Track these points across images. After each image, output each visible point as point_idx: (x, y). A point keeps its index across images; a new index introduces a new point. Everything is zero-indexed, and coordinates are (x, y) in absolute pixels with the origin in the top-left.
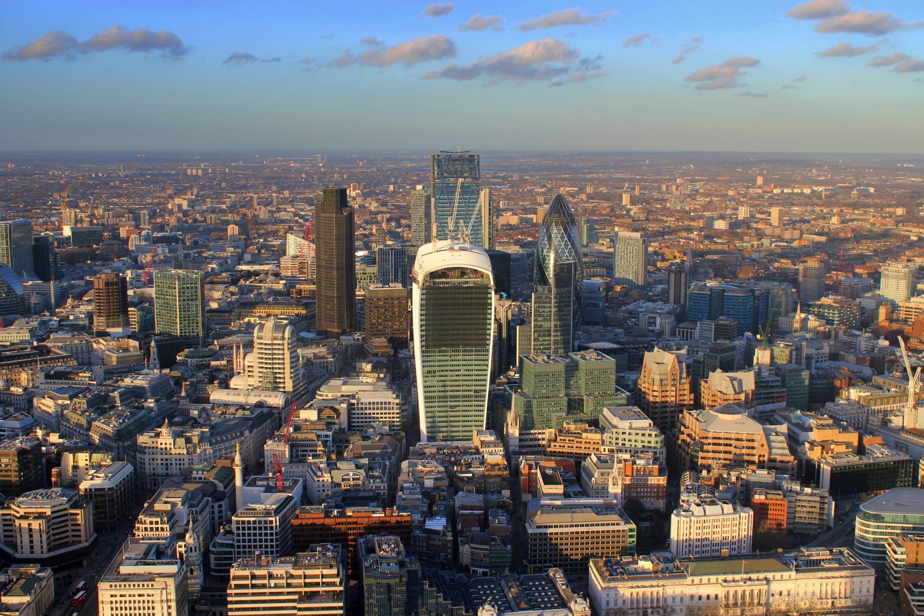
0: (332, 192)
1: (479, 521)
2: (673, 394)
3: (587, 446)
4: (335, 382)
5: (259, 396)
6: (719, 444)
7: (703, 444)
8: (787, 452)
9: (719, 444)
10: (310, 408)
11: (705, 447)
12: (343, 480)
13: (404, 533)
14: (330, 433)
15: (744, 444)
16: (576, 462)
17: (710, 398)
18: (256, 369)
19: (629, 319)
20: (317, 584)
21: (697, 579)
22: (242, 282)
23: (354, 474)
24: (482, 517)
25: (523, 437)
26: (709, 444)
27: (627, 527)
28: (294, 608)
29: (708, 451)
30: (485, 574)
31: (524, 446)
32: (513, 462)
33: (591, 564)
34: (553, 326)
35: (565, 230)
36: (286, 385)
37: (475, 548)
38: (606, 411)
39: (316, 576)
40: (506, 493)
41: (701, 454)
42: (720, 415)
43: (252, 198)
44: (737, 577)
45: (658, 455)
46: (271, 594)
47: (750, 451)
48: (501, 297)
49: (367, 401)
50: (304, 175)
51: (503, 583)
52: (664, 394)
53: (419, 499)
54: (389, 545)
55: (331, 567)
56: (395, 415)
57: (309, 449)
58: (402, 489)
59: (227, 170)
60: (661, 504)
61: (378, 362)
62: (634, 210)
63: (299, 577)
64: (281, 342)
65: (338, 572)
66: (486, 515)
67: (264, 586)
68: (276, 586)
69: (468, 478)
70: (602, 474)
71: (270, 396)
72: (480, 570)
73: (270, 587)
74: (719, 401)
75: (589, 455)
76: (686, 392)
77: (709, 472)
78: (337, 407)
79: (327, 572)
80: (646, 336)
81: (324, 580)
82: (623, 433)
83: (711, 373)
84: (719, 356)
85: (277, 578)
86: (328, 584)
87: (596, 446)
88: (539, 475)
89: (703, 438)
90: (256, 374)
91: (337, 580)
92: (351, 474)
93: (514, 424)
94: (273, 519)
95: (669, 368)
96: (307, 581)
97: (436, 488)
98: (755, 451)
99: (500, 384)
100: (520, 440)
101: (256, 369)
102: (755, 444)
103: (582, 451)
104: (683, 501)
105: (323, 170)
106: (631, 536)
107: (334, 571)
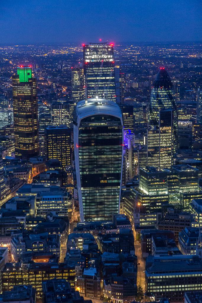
53: (79, 257)
54: (62, 286)
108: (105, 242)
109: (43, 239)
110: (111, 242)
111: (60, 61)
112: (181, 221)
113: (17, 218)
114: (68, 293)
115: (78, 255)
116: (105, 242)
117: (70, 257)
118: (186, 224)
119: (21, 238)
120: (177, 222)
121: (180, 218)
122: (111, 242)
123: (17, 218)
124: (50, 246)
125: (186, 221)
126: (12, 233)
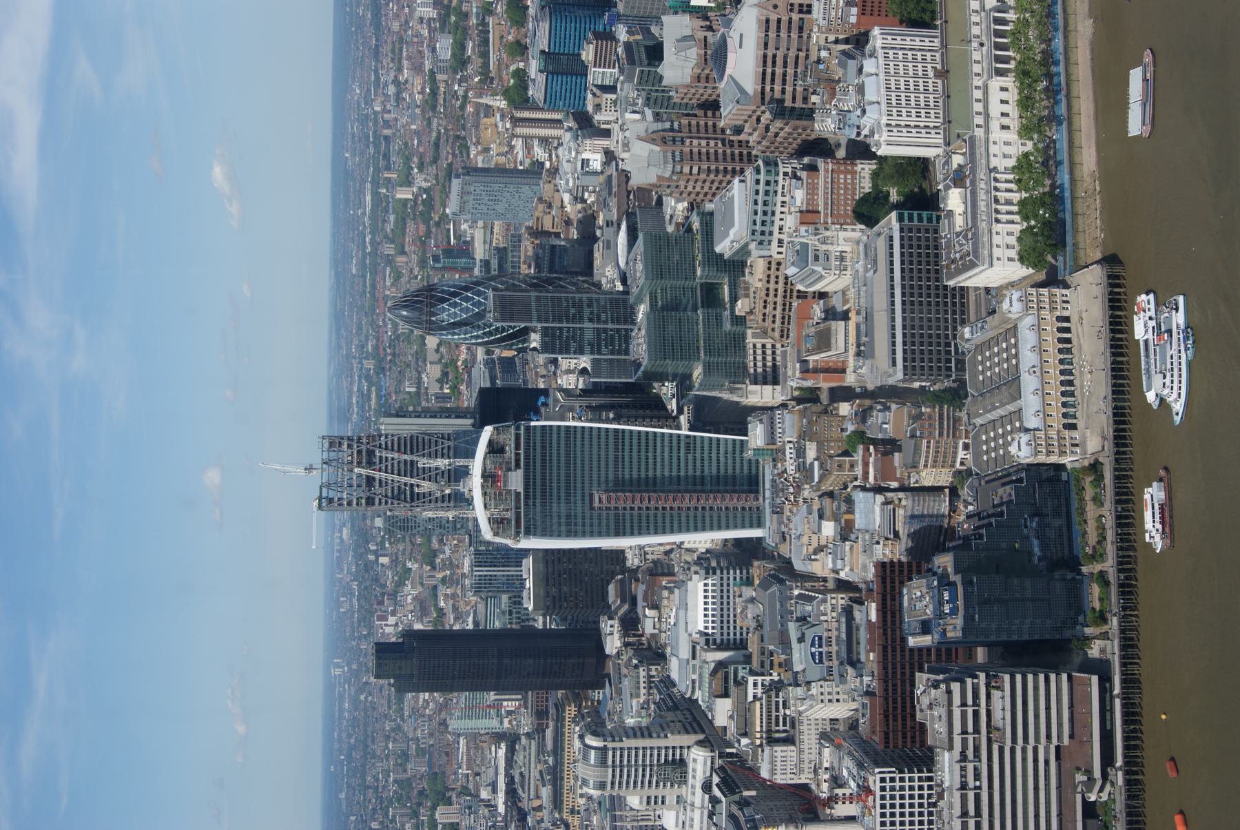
0: (379, 665)
1: (885, 454)
2: (695, 142)
3: (773, 279)
5: (693, 787)
6: (773, 74)
7: (772, 99)
9: (773, 74)
10: (711, 710)
11: (777, 95)
13: (901, 571)
14: (751, 680)
15: (772, 34)
16: (798, 297)
17: (702, 84)
18: (653, 792)
19: (583, 201)
20: (976, 714)
21: (979, 120)
22: (525, 804)
24: (881, 448)
26: (772, 90)
27: (896, 226)
28: (1013, 750)
29: (783, 92)
30: (966, 447)
33: (951, 283)
35: (443, 300)
36: (677, 744)
37: (926, 461)
38: (718, 249)
39: (964, 715)
40: (845, 408)
41: (788, 103)
42: (728, 71)
43: (395, 781)
44: (976, 56)
45: (789, 170)
46: (990, 787)
47: (784, 26)
48: (545, 404)
49: (701, 618)
50: (362, 697)
51: (979, 421)
52: (696, 157)
53: (852, 547)
55: (949, 692)
56: (725, 576)
57: (774, 714)
59: (353, 818)
60: (865, 169)
61: (645, 599)
62: (421, 181)
63: (964, 742)
64: (610, 753)
65: (955, 680)
66: (874, 442)
67: (977, 798)
68: (977, 776)
69: (821, 467)
70: (817, 258)
71: (694, 770)
72: (961, 454)
73: (979, 788)
74: (707, 71)
75: (786, 278)
76: (694, 122)
78: (713, 665)
79: (957, 700)
80: (610, 177)
81: (970, 702)
82: (755, 223)
83: (664, 83)
85: (963, 776)
86: (976, 695)
87: (774, 266)
88: (816, 357)
89: (763, 99)
90: (660, 792)
91: (969, 681)
92: (813, 650)
94: (878, 776)
95: (657, 148)
96: (970, 729)
98: (785, 19)
99: (680, 411)
100: (765, 383)
101: (653, 792)
102: (774, 17)
104: (858, 134)
105: (354, 667)
106: (911, 219)
107: (956, 687)
108: (816, 479)
109: (803, 634)
110: (816, 463)
111: (372, 557)
112: (768, 282)
113: (750, 698)
114: (936, 583)
115: (847, 548)
116: (816, 479)
117: (852, 570)
119: (799, 691)
120: (772, 293)
121: (759, 285)
122: (816, 463)
123: (750, 698)
124: (822, 618)
125: (769, 269)
126: (788, 712)
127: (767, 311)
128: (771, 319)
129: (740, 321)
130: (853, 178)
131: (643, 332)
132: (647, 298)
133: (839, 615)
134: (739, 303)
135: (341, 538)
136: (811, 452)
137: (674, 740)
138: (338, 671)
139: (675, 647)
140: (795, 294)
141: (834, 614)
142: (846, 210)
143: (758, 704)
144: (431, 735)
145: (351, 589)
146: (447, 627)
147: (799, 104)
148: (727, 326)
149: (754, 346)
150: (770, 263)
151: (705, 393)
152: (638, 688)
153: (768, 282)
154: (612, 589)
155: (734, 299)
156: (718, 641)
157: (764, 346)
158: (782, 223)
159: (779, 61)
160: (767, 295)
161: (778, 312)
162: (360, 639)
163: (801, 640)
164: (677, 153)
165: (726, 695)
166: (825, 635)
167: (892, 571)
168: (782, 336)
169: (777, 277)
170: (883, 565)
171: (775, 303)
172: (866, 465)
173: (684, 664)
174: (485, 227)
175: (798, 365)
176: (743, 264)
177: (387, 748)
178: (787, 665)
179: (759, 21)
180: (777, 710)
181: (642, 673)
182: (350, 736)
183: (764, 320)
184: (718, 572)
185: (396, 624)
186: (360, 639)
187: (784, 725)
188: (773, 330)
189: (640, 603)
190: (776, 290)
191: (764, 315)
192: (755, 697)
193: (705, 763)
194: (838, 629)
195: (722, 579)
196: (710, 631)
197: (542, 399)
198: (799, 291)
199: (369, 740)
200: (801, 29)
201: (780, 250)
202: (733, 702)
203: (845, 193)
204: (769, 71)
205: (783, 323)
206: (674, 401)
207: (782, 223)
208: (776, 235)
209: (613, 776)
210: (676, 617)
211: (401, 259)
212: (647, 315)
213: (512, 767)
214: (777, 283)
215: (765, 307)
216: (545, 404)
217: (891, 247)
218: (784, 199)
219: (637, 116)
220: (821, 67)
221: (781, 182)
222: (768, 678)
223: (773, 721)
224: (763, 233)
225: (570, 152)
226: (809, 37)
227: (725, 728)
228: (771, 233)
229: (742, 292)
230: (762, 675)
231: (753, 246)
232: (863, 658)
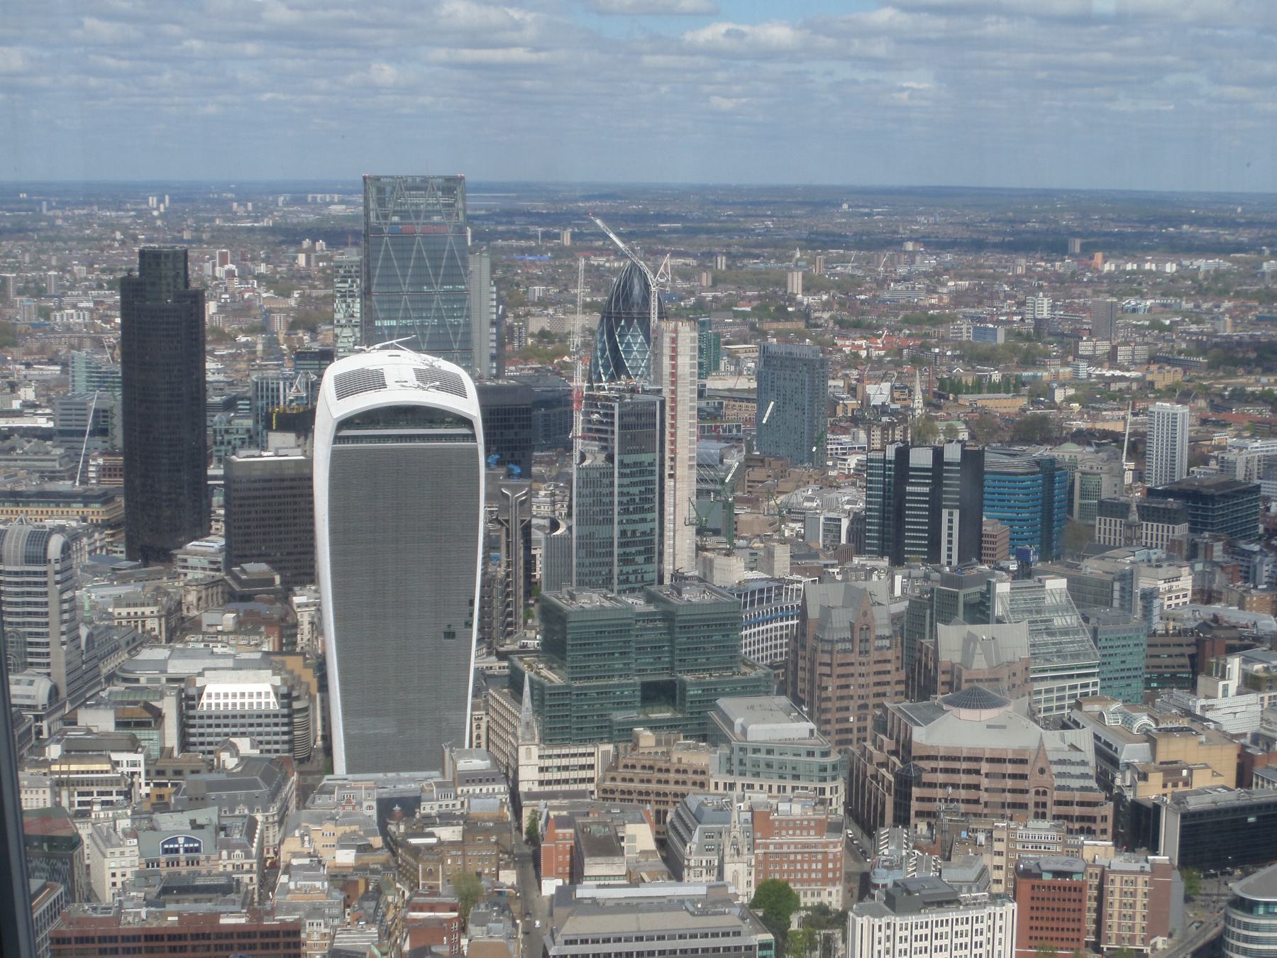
3: (681, 777)
4: (160, 653)
8: (1093, 783)
9: (954, 771)
10: (98, 705)
12: (166, 851)
14: (140, 757)
16: (658, 812)
23: (188, 840)
24: (456, 926)
25: (548, 763)
26: (934, 770)
29: (931, 785)
31: (549, 782)
32: (526, 813)
34: (616, 534)
57: (95, 789)
58: (288, 869)
60: (834, 897)
69: (430, 848)
75: (683, 796)
77: (929, 825)
80: (816, 556)
82: (756, 751)
83: (940, 626)
84: (962, 593)
87: (699, 778)
92: (181, 840)
93: (528, 737)
97: (360, 868)
100: (541, 769)
103: (671, 788)
105: (159, 223)
108: (414, 841)
110: (433, 841)
112: (678, 771)
113: (115, 757)
116: (414, 841)
118: (694, 783)
120: (663, 776)
121: (675, 759)
123: (115, 757)
124: (224, 853)
125: (695, 772)
126: (97, 808)
127: (638, 770)
128: (628, 776)
129: (624, 734)
130: (816, 881)
131: (607, 604)
132: (652, 608)
133: (228, 875)
134: (648, 733)
135: (332, 203)
136: (449, 834)
137: (59, 654)
138: (153, 201)
139: (184, 654)
140: (662, 807)
141: (230, 868)
142: (775, 872)
143: (107, 767)
144: (68, 328)
145: (263, 216)
146: (208, 348)
147: (915, 806)
148: (619, 716)
149: (592, 754)
150: (703, 773)
151: (527, 689)
152: (128, 605)
153: (678, 771)
154: (263, 567)
155: (654, 726)
156: (192, 712)
157: (591, 767)
158: (757, 787)
159: (972, 779)
160: (660, 770)
161: (636, 786)
162: (196, 230)
163: (195, 825)
164: (848, 646)
165: (119, 724)
166: (202, 857)
167: (288, 945)
168: (605, 791)
169: (684, 783)
170: (297, 933)
171: (649, 781)
172: (432, 908)
173: (161, 666)
174: (749, 391)
175: (564, 813)
176: (704, 738)
177: (49, 269)
178: (161, 805)
179: (1024, 750)
180: (100, 794)
181: (147, 610)
182: (65, 219)
183: (626, 766)
184: (285, 711)
185: (215, 278)
186: (196, 230)
187: (80, 803)
188: (613, 779)
189: (243, 606)
190: (667, 782)
191: (633, 767)
192: (117, 763)
193: (28, 697)
194: (209, 874)
195: (276, 716)
196: (204, 700)
197: (517, 470)
198: (666, 813)
199: (61, 244)
200: (1014, 805)
201: (721, 786)
202: (107, 734)
203: (802, 871)
204: (956, 765)
205: (623, 792)
206: (516, 647)
207: (757, 787)
208: (739, 781)
209: (9, 573)
210: (224, 656)
211: (706, 279)
212: (630, 608)
213: (22, 436)
214: (677, 782)
215: (644, 767)
216: (509, 475)
217: (726, 934)
218: (789, 789)
219: (898, 592)
220: (964, 834)
221: (811, 786)
222: (143, 780)
223: (86, 789)
224: (741, 762)
225: (849, 502)
226: (1003, 817)
227: (75, 724)
228: (742, 774)
229: (664, 735)
230: (147, 773)
231: (723, 750)
232: (171, 907)
